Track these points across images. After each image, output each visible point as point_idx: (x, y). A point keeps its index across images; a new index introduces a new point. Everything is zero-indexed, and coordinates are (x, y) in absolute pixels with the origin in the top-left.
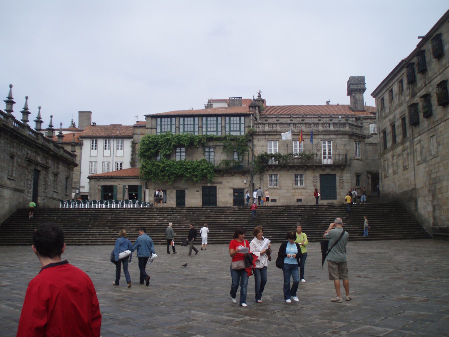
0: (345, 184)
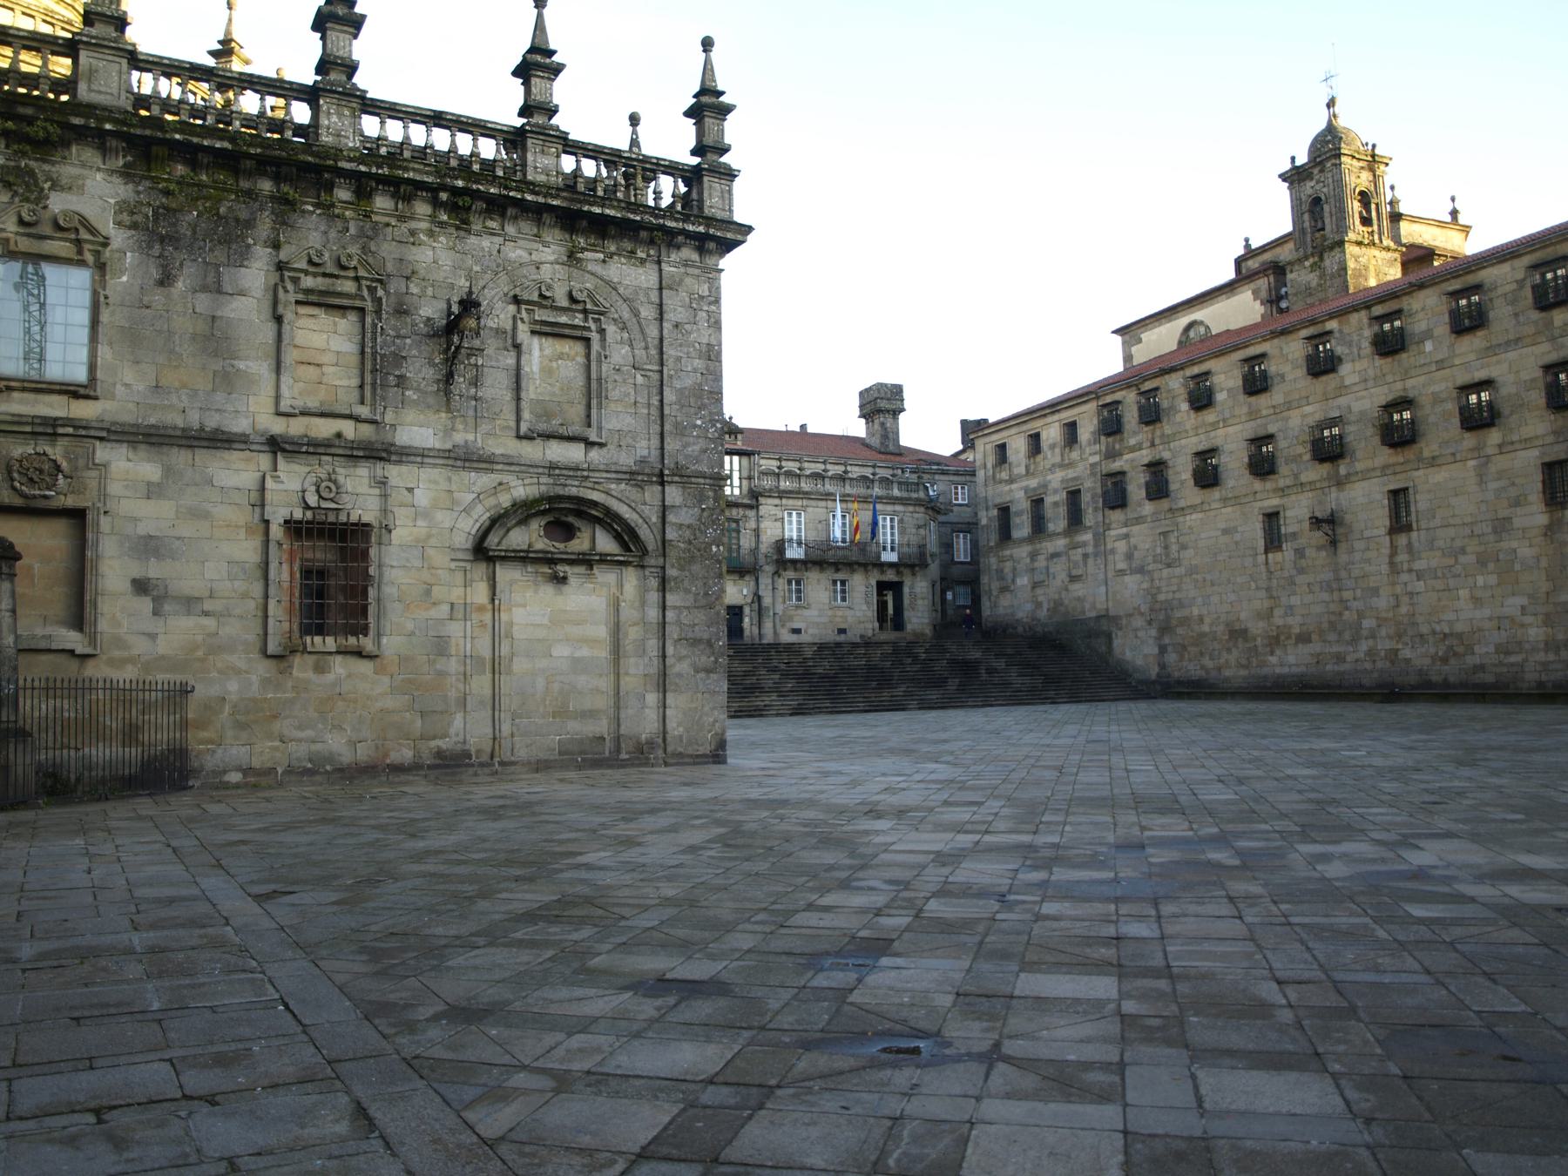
0: (920, 602)
